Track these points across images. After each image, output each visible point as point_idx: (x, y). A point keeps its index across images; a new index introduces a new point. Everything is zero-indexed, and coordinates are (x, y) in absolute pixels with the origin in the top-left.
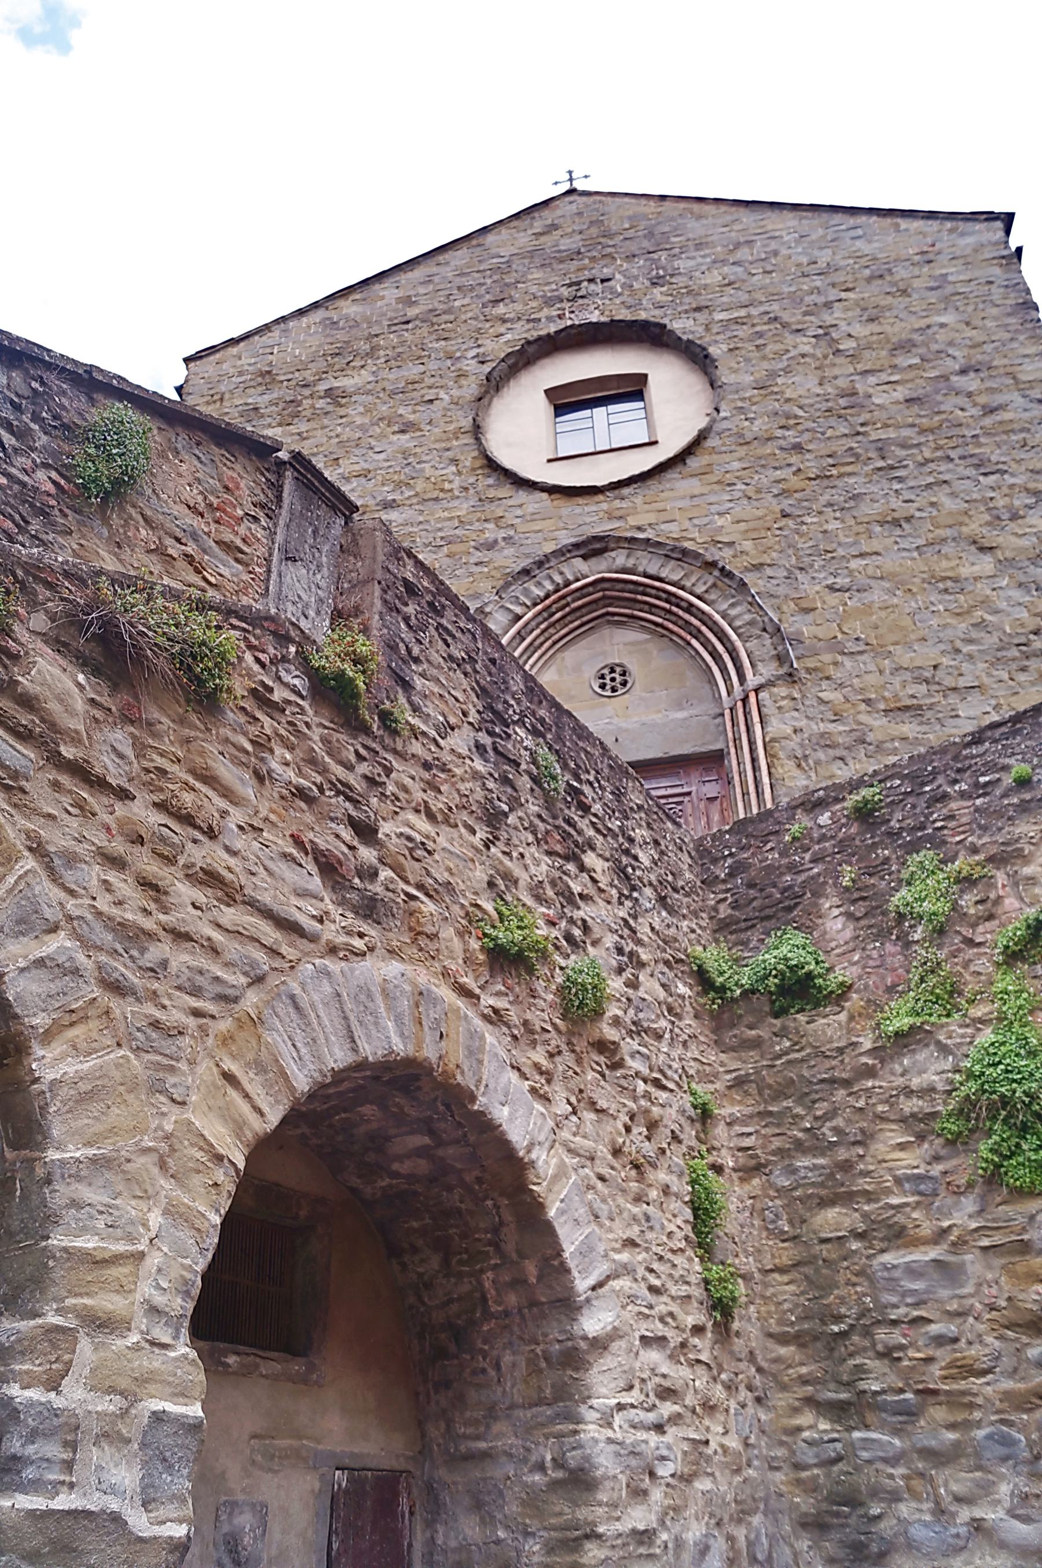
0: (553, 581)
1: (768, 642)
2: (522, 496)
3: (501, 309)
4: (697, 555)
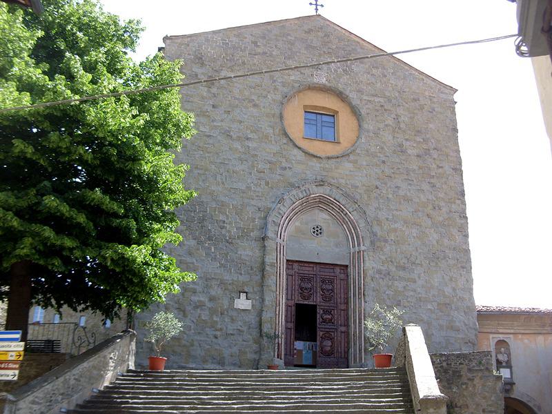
2: (296, 151)
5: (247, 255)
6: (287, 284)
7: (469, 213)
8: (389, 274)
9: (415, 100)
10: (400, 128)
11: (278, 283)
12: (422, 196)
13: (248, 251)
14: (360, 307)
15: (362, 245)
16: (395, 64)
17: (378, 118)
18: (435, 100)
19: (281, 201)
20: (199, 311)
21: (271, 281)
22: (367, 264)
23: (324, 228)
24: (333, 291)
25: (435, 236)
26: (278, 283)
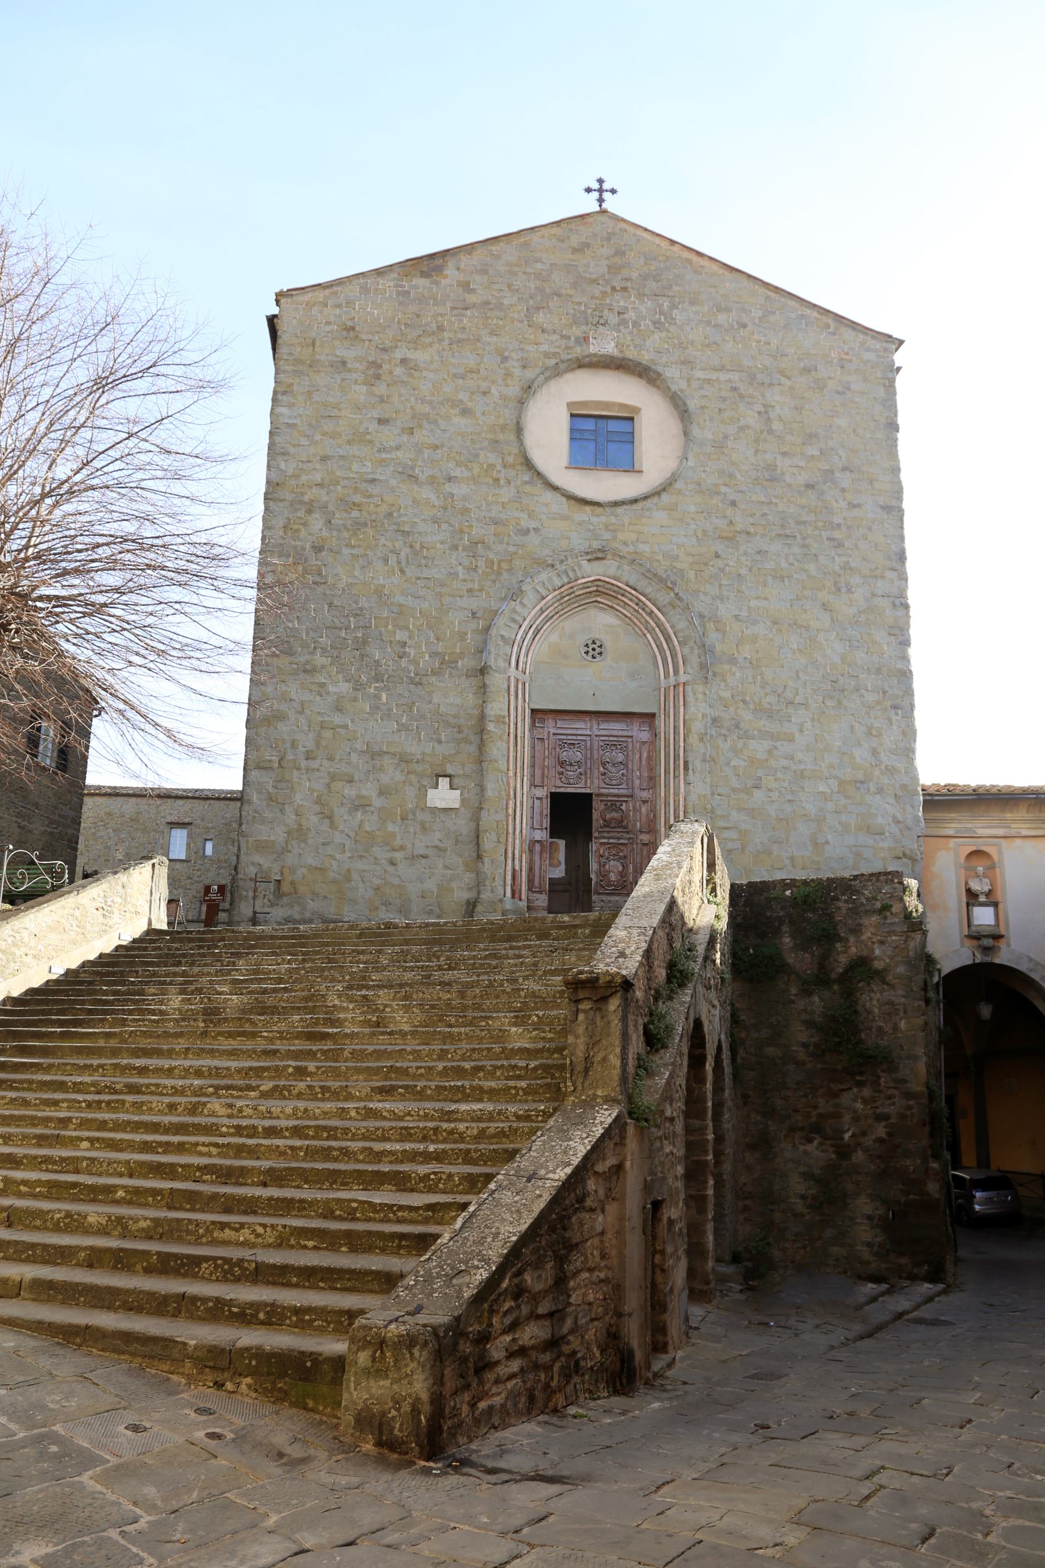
0: (568, 576)
1: (696, 651)
2: (549, 496)
3: (540, 318)
6: (533, 757)
8: (737, 727)
9: (806, 371)
11: (512, 754)
12: (812, 567)
13: (452, 696)
14: (676, 794)
15: (681, 671)
16: (767, 298)
20: (359, 815)
21: (496, 750)
22: (692, 709)
23: (608, 644)
26: (512, 754)
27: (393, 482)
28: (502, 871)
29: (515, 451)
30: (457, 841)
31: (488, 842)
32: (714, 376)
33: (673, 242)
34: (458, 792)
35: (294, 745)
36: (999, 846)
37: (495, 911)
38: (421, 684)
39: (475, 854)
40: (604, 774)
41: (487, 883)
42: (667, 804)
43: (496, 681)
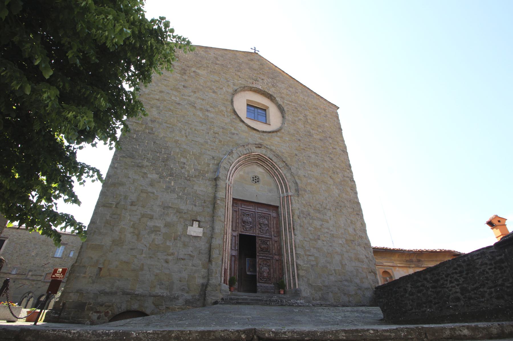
2: (241, 124)
3: (239, 73)
4: (281, 158)
5: (202, 191)
6: (233, 218)
7: (355, 178)
8: (309, 215)
10: (307, 122)
12: (325, 165)
13: (202, 188)
17: (295, 114)
18: (327, 111)
19: (231, 153)
20: (153, 236)
21: (220, 212)
22: (294, 206)
24: (269, 227)
25: (337, 191)
27: (186, 106)
28: (220, 269)
29: (231, 108)
30: (200, 252)
31: (215, 254)
32: (290, 103)
33: (276, 67)
34: (202, 229)
35: (126, 198)
36: (391, 269)
37: (217, 290)
38: (190, 180)
39: (208, 260)
40: (260, 228)
41: (213, 275)
42: (286, 243)
43: (221, 184)
